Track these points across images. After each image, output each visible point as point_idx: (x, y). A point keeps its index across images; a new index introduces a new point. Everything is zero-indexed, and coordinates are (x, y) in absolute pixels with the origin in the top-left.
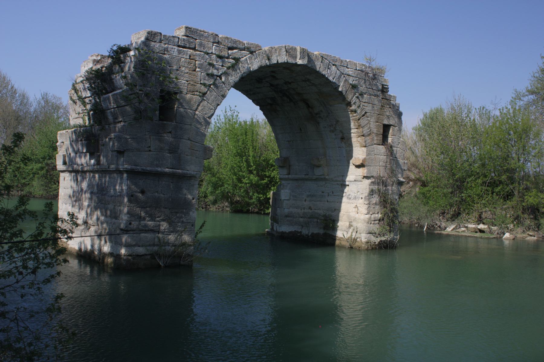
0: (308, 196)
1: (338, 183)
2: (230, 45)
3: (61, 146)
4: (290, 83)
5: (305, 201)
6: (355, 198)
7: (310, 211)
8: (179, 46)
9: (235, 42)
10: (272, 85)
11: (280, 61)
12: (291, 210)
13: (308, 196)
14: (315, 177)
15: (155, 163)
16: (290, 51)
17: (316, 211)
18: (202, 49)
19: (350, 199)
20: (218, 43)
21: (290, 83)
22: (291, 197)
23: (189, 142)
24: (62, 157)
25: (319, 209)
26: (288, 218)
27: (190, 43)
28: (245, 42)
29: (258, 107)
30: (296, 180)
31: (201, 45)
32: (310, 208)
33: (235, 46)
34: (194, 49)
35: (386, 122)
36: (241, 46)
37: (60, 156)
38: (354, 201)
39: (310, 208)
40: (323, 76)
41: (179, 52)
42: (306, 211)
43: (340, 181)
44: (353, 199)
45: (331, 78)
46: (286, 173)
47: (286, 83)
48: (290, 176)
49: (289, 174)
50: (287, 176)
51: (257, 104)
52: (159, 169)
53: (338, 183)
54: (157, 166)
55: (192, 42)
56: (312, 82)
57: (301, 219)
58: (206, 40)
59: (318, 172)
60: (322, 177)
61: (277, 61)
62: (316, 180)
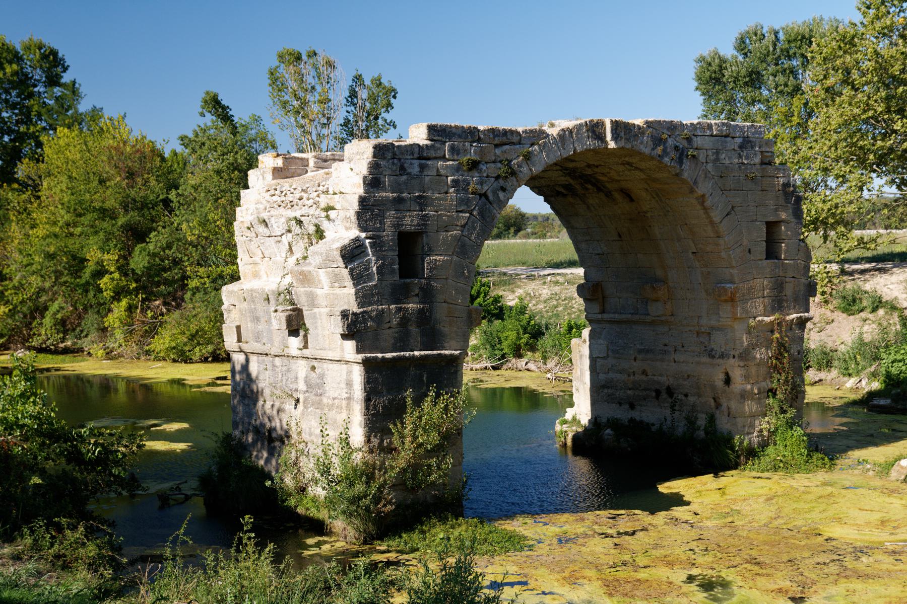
0: (640, 351)
1: (692, 328)
2: (497, 141)
3: (229, 311)
4: (597, 167)
5: (635, 360)
6: (722, 356)
7: (644, 377)
8: (419, 158)
9: (505, 132)
12: (611, 375)
13: (640, 351)
14: (649, 319)
16: (595, 129)
17: (655, 378)
19: (713, 357)
20: (479, 140)
21: (597, 167)
22: (610, 353)
23: (444, 305)
24: (235, 329)
25: (661, 375)
26: (606, 391)
28: (520, 130)
29: (542, 198)
30: (619, 322)
31: (453, 149)
32: (644, 373)
33: (504, 139)
34: (443, 158)
35: (771, 219)
36: (515, 139)
37: (230, 328)
38: (720, 361)
39: (644, 373)
41: (422, 167)
42: (639, 377)
43: (694, 326)
44: (719, 357)
46: (598, 311)
47: (589, 166)
48: (605, 316)
49: (603, 312)
50: (600, 316)
51: (539, 194)
52: (407, 354)
53: (692, 328)
55: (439, 149)
57: (629, 392)
59: (655, 310)
60: (663, 318)
61: (575, 150)
62: (652, 323)
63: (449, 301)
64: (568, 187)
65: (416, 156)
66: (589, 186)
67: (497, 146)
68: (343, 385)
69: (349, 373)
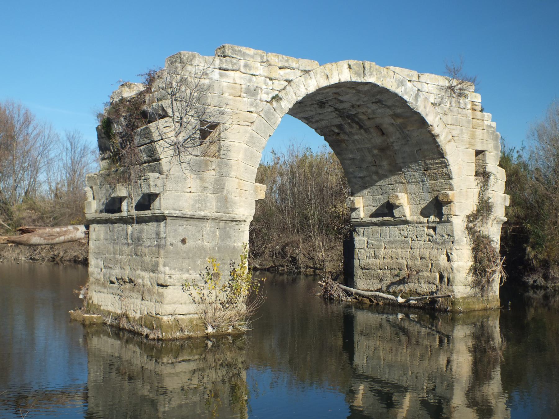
0: (389, 242)
8: (220, 69)
10: (336, 109)
11: (343, 80)
15: (197, 206)
18: (248, 72)
23: (237, 180)
27: (233, 64)
29: (323, 137)
31: (246, 66)
33: (286, 64)
35: (480, 148)
40: (396, 95)
41: (221, 76)
45: (406, 97)
47: (353, 106)
54: (200, 209)
55: (235, 64)
56: (384, 103)
58: (252, 59)
63: (239, 178)
64: (340, 127)
65: (217, 66)
66: (354, 125)
67: (280, 68)
68: (154, 236)
69: (159, 226)
